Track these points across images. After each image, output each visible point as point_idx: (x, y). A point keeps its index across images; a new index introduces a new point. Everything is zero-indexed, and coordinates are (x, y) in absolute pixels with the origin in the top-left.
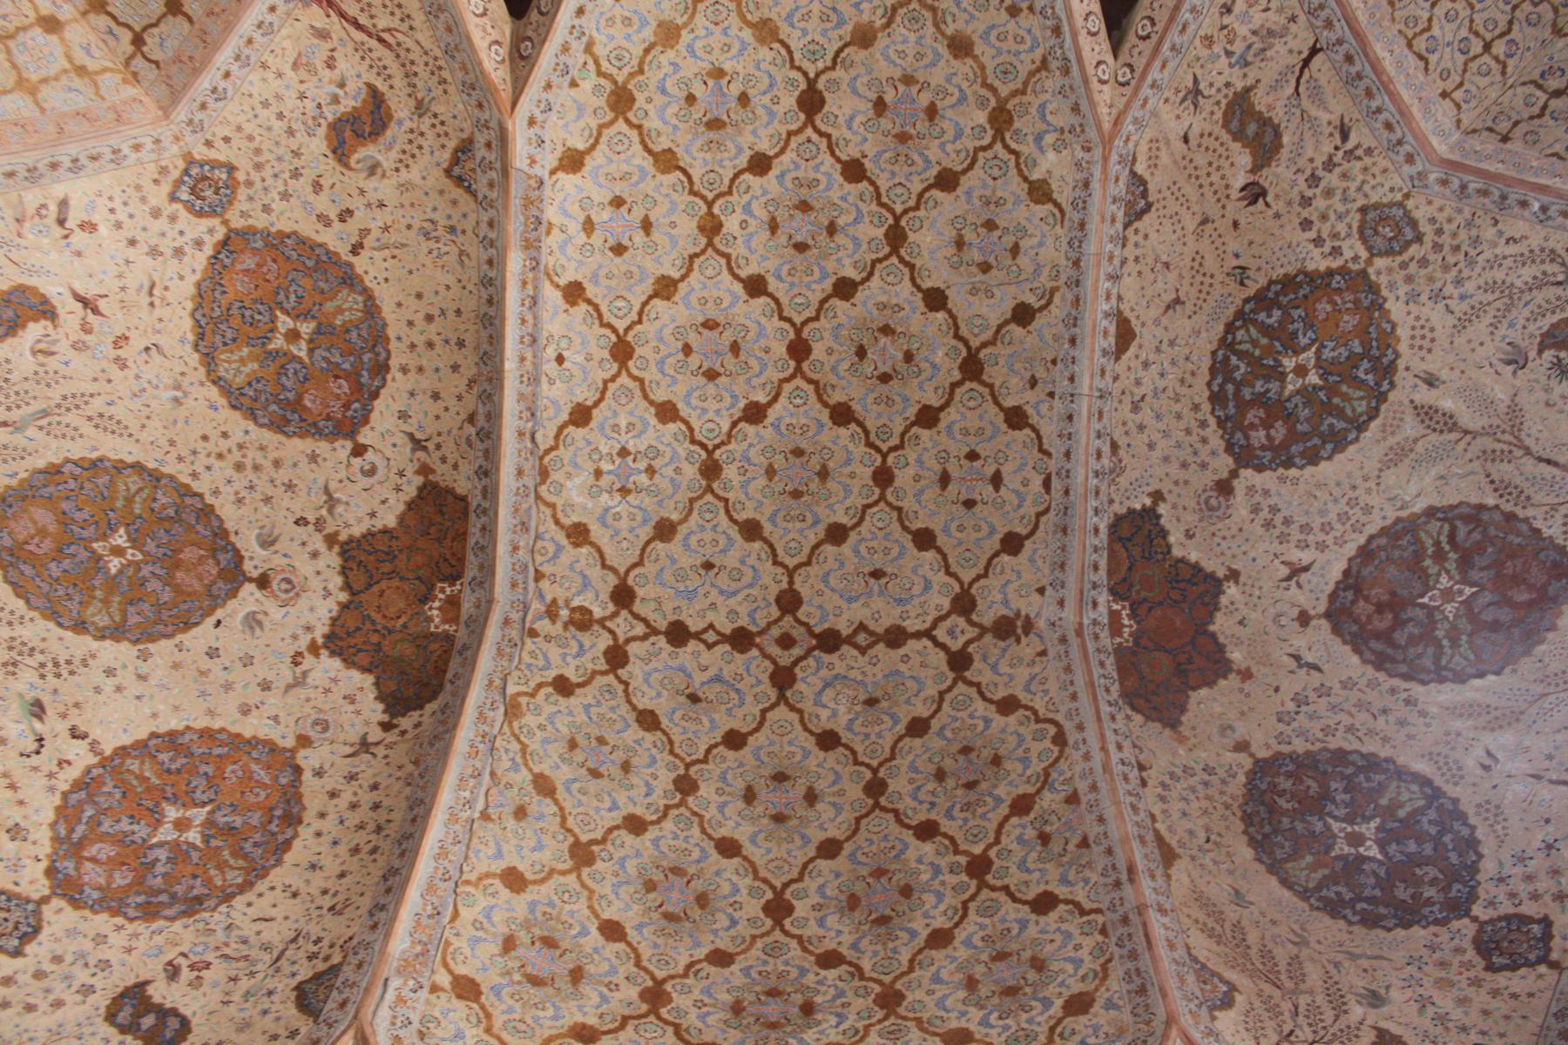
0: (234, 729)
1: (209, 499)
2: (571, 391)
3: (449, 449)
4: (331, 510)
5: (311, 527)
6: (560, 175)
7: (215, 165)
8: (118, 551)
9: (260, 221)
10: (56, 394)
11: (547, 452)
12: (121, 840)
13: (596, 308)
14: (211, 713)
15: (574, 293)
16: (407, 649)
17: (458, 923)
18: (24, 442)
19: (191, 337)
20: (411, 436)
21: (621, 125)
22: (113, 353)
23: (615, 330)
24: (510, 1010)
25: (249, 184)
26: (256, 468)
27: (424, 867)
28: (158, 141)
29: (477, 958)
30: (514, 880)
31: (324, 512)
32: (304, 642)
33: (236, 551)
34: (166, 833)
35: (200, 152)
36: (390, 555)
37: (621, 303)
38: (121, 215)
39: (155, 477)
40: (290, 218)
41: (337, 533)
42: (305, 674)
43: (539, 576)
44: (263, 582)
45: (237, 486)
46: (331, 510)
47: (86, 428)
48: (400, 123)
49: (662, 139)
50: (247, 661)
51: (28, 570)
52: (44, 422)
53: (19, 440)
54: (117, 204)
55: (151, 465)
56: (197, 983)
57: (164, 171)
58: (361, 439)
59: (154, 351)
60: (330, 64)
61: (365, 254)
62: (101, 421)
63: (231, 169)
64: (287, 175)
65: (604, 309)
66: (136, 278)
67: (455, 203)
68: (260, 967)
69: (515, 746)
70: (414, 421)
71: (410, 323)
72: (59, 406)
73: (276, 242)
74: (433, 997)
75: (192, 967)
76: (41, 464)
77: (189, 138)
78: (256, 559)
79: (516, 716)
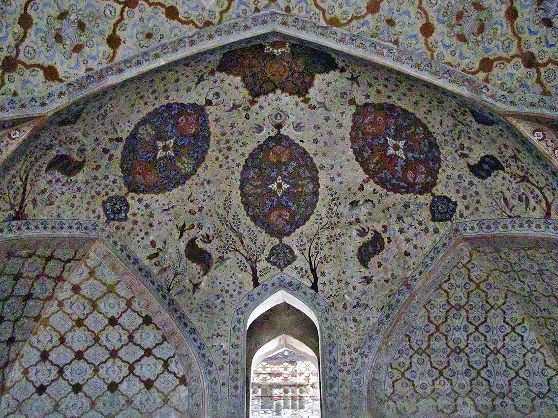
0: (350, 129)
1: (247, 156)
2: (162, 23)
3: (201, 67)
4: (239, 106)
5: (249, 112)
6: (60, 76)
7: (105, 210)
8: (279, 186)
9: (121, 182)
10: (223, 228)
11: (196, 26)
12: (405, 169)
13: (115, 25)
14: (343, 139)
15: (114, 41)
16: (300, 62)
17: (453, 64)
18: (246, 232)
19: (180, 188)
20: (197, 84)
21: (21, 57)
22: (198, 214)
23: (122, 11)
24: (497, 47)
25: (107, 193)
26: (227, 142)
27: (426, 77)
28: (108, 237)
29: (471, 57)
30: (427, 30)
31: (240, 109)
32: (302, 105)
33: (266, 141)
34: (401, 153)
35: (104, 219)
36: (254, 75)
37: (108, 12)
38: (142, 234)
39: (244, 181)
40: (115, 171)
41: (249, 101)
42: (319, 103)
43: (257, 10)
44: (279, 127)
45: (237, 147)
46: (239, 106)
47: (232, 212)
48: (59, 151)
49: (17, 31)
50: (317, 127)
51: (297, 218)
52: (235, 228)
53: (246, 234)
54: (138, 238)
55: (239, 183)
56: (470, 150)
57: (118, 228)
58: (204, 103)
59: (192, 198)
60: (44, 191)
61: (120, 135)
62: (227, 206)
63: (104, 203)
64: (97, 181)
65: (114, 21)
66: (164, 218)
67: (87, 113)
68: (465, 129)
69: (354, 22)
70: (190, 85)
71: (146, 103)
72: (227, 225)
73: (127, 171)
74: (493, 82)
75: (463, 149)
76: (252, 224)
77: (101, 226)
78: (269, 131)
79: (338, 21)
